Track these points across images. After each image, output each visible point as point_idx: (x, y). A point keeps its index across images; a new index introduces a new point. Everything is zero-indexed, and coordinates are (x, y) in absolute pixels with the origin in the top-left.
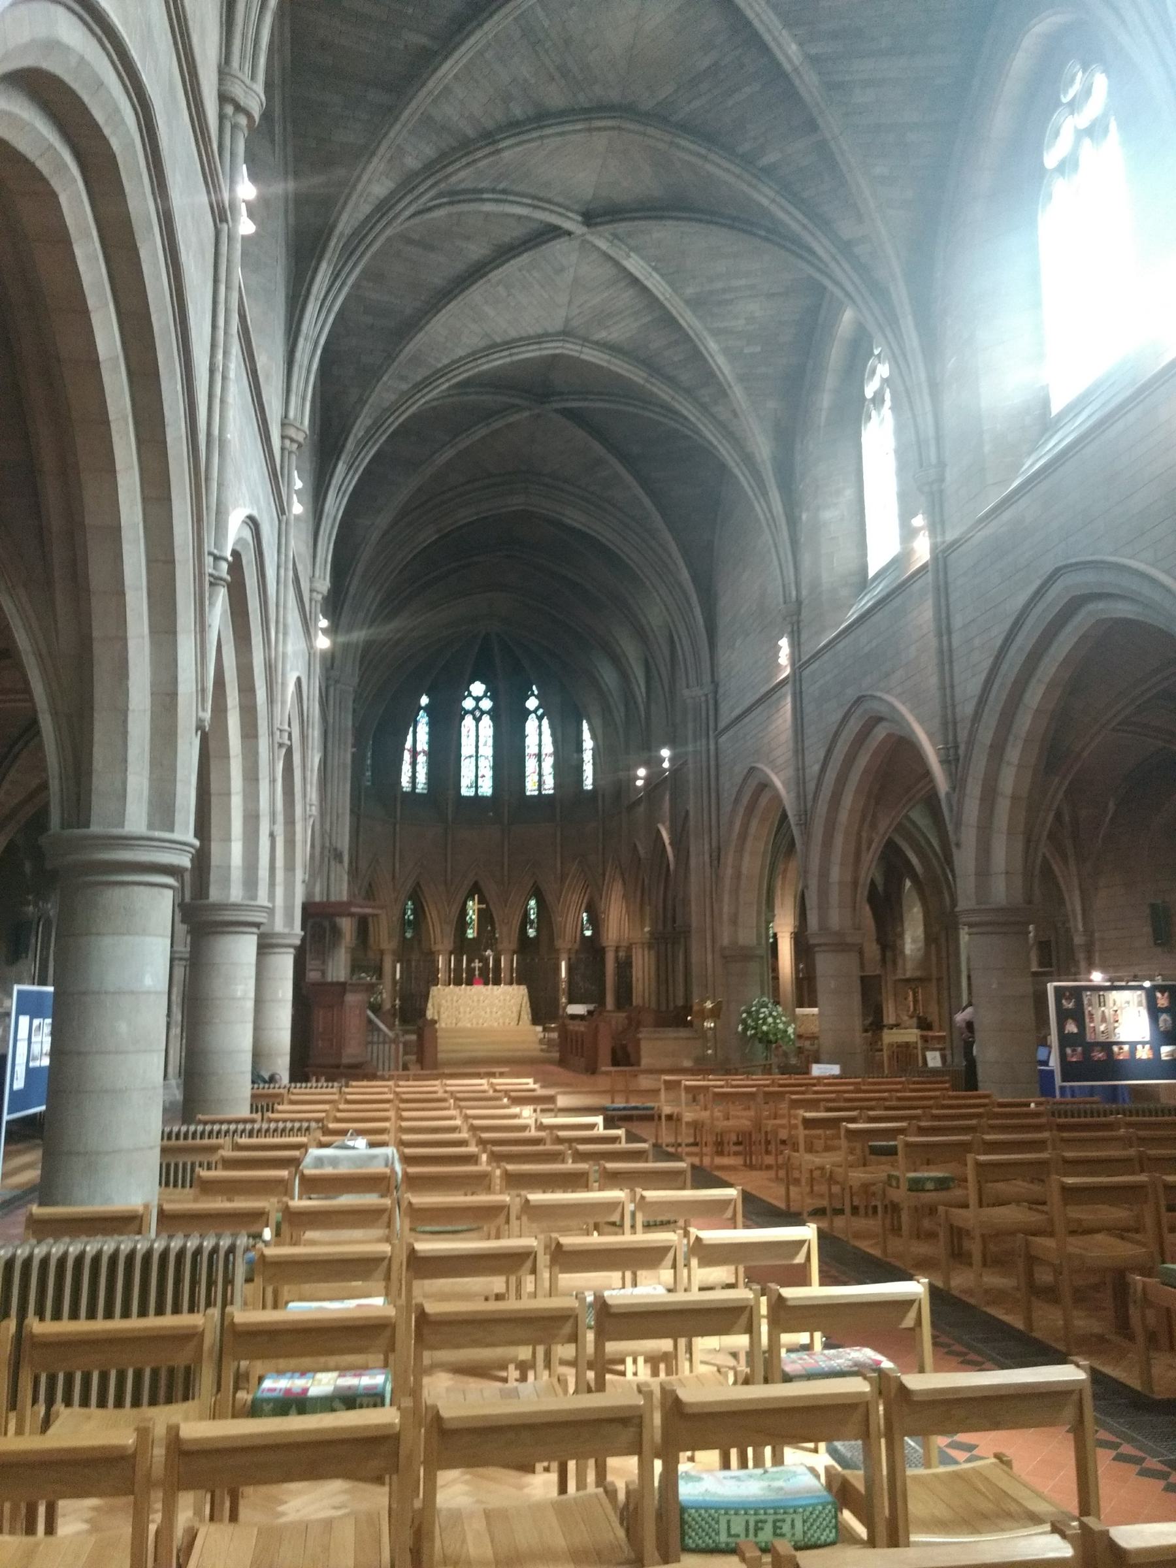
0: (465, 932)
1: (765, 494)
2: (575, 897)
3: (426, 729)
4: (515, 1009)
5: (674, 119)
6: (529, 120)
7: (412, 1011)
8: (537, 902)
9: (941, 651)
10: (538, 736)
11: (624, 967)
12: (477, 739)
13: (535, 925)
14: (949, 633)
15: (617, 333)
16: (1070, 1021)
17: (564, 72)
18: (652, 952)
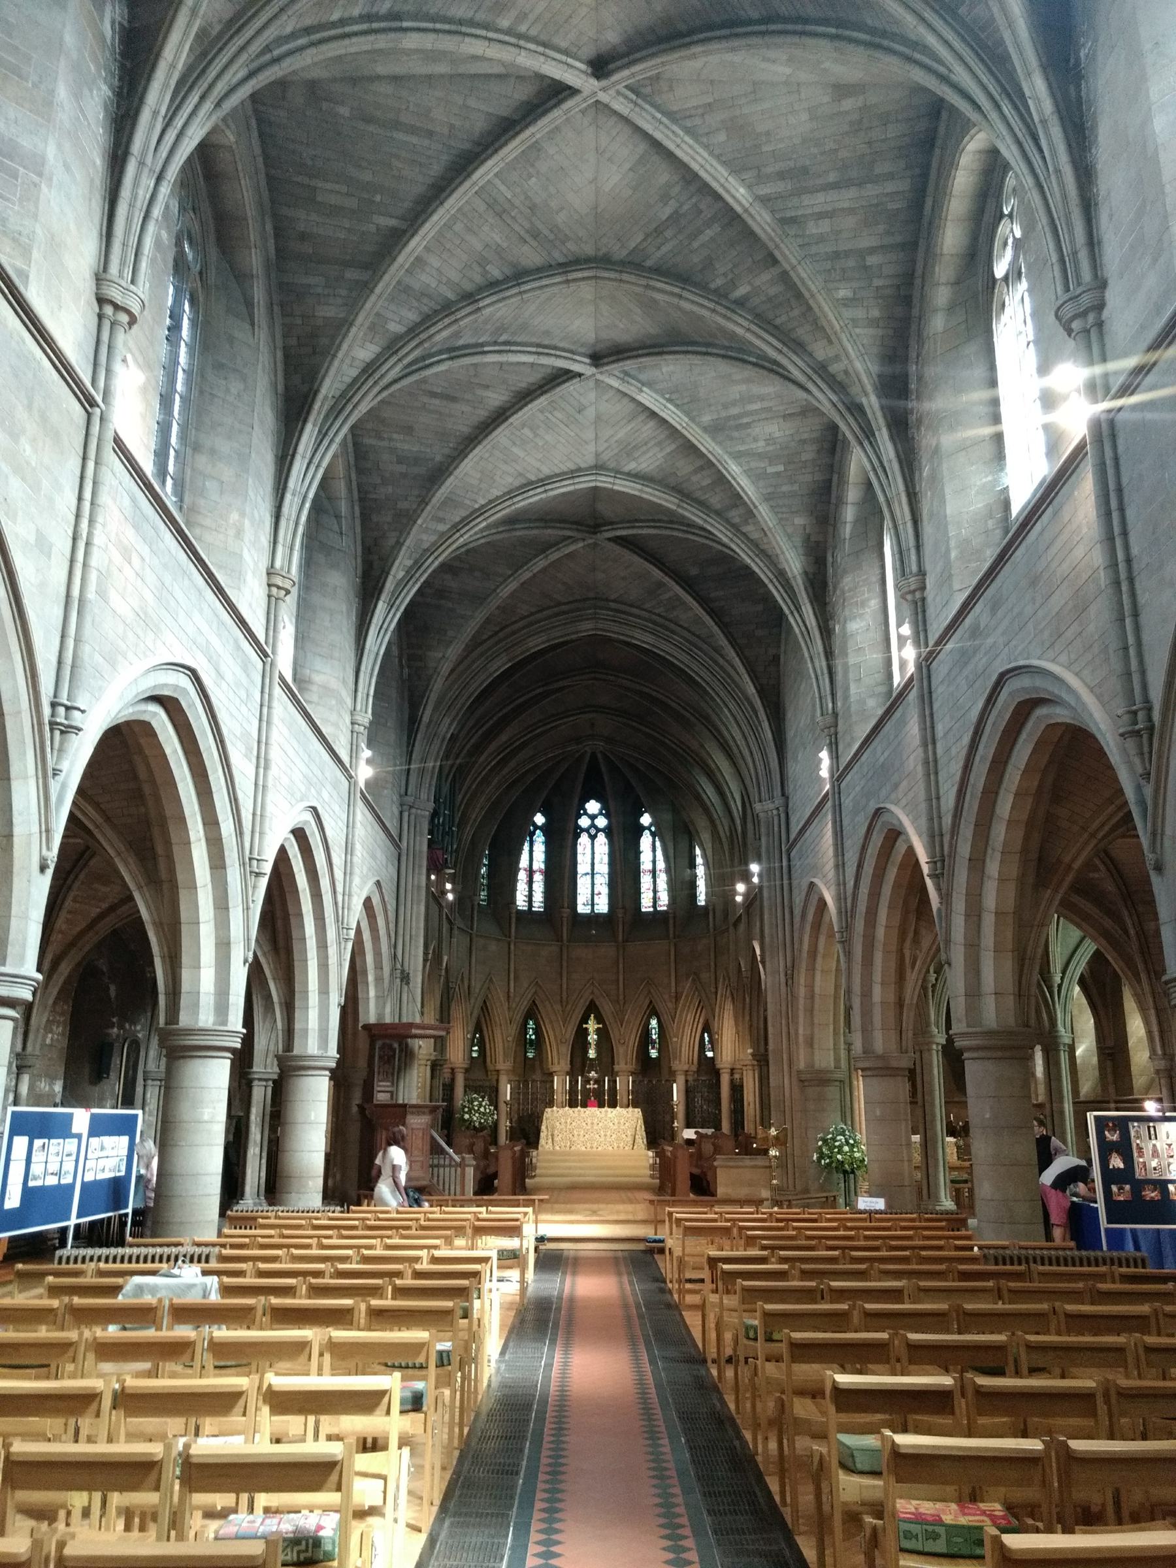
1: (798, 608)
2: (690, 1018)
5: (649, 263)
6: (507, 279)
7: (528, 1132)
8: (659, 1022)
9: (926, 762)
10: (650, 852)
11: (737, 1090)
12: (593, 856)
14: (934, 743)
15: (649, 460)
16: (1114, 1155)
17: (536, 235)
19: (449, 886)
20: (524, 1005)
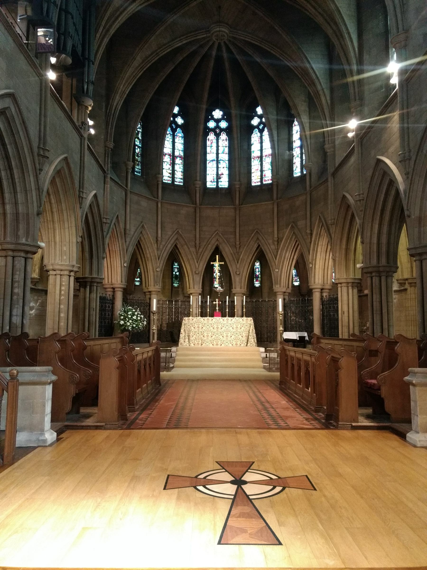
2: (288, 254)
4: (244, 335)
7: (171, 335)
8: (261, 265)
12: (217, 151)
18: (356, 291)
19: (91, 123)
20: (169, 247)
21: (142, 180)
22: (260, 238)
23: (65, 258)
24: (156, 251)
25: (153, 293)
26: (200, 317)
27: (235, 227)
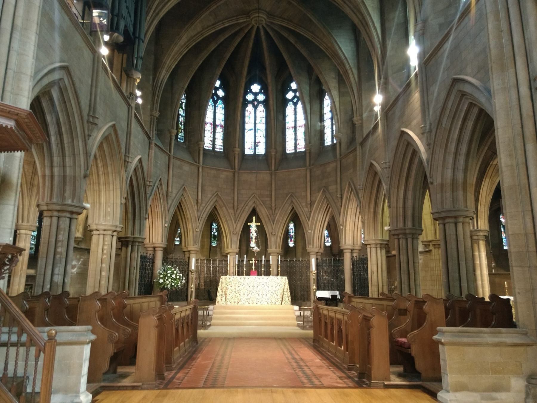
0: (250, 243)
3: (223, 112)
4: (280, 293)
7: (209, 294)
12: (255, 120)
13: (293, 239)
18: (384, 252)
19: (139, 93)
20: (209, 209)
21: (185, 147)
22: (294, 201)
23: (109, 218)
24: (196, 213)
25: (192, 252)
26: (236, 276)
27: (271, 191)
